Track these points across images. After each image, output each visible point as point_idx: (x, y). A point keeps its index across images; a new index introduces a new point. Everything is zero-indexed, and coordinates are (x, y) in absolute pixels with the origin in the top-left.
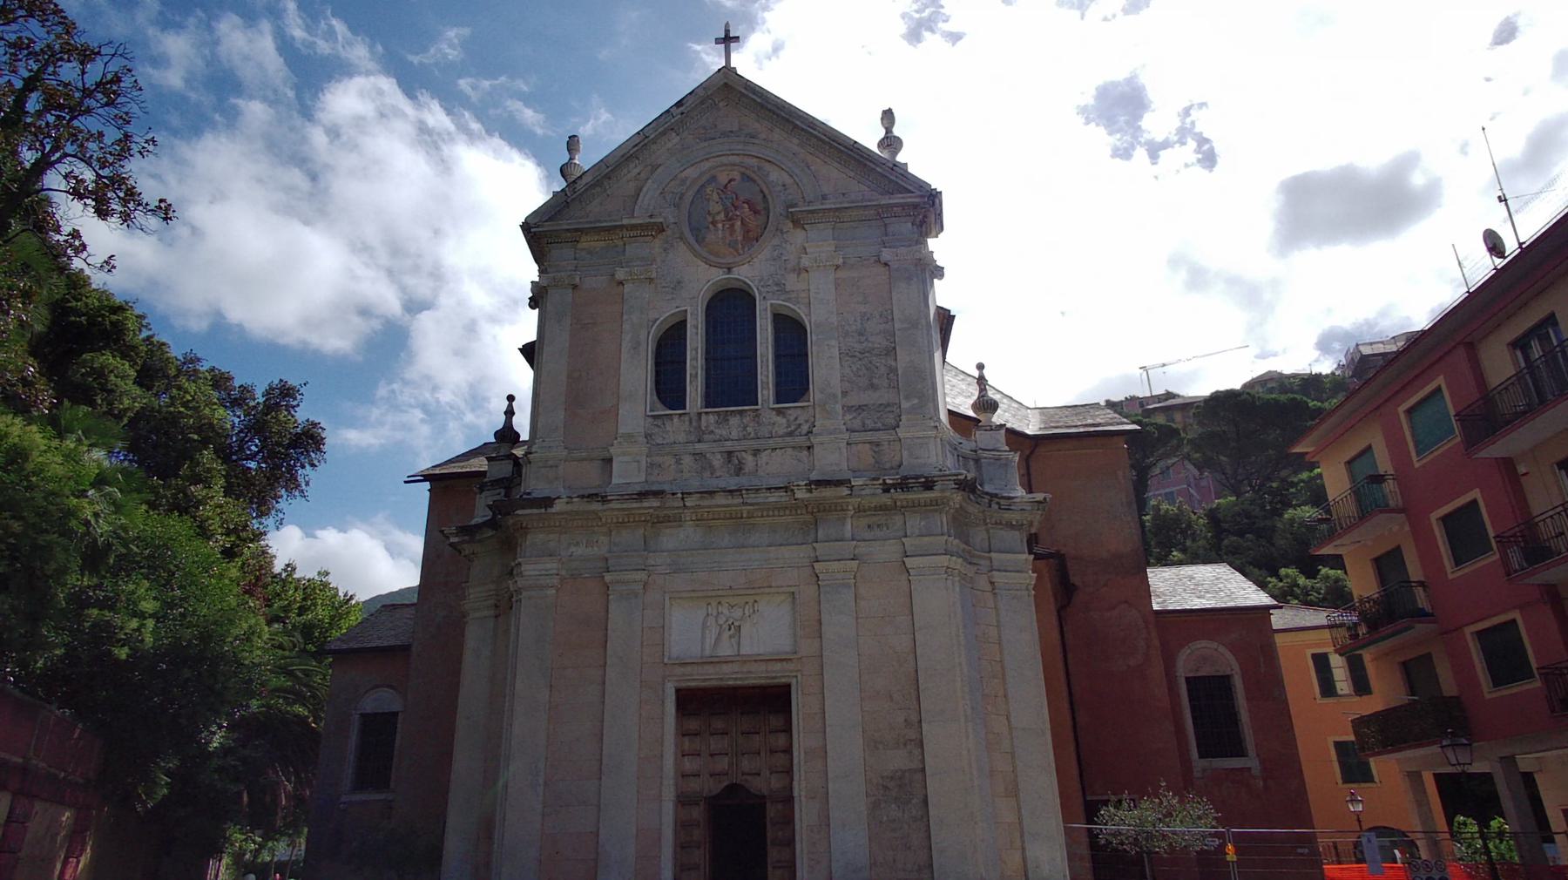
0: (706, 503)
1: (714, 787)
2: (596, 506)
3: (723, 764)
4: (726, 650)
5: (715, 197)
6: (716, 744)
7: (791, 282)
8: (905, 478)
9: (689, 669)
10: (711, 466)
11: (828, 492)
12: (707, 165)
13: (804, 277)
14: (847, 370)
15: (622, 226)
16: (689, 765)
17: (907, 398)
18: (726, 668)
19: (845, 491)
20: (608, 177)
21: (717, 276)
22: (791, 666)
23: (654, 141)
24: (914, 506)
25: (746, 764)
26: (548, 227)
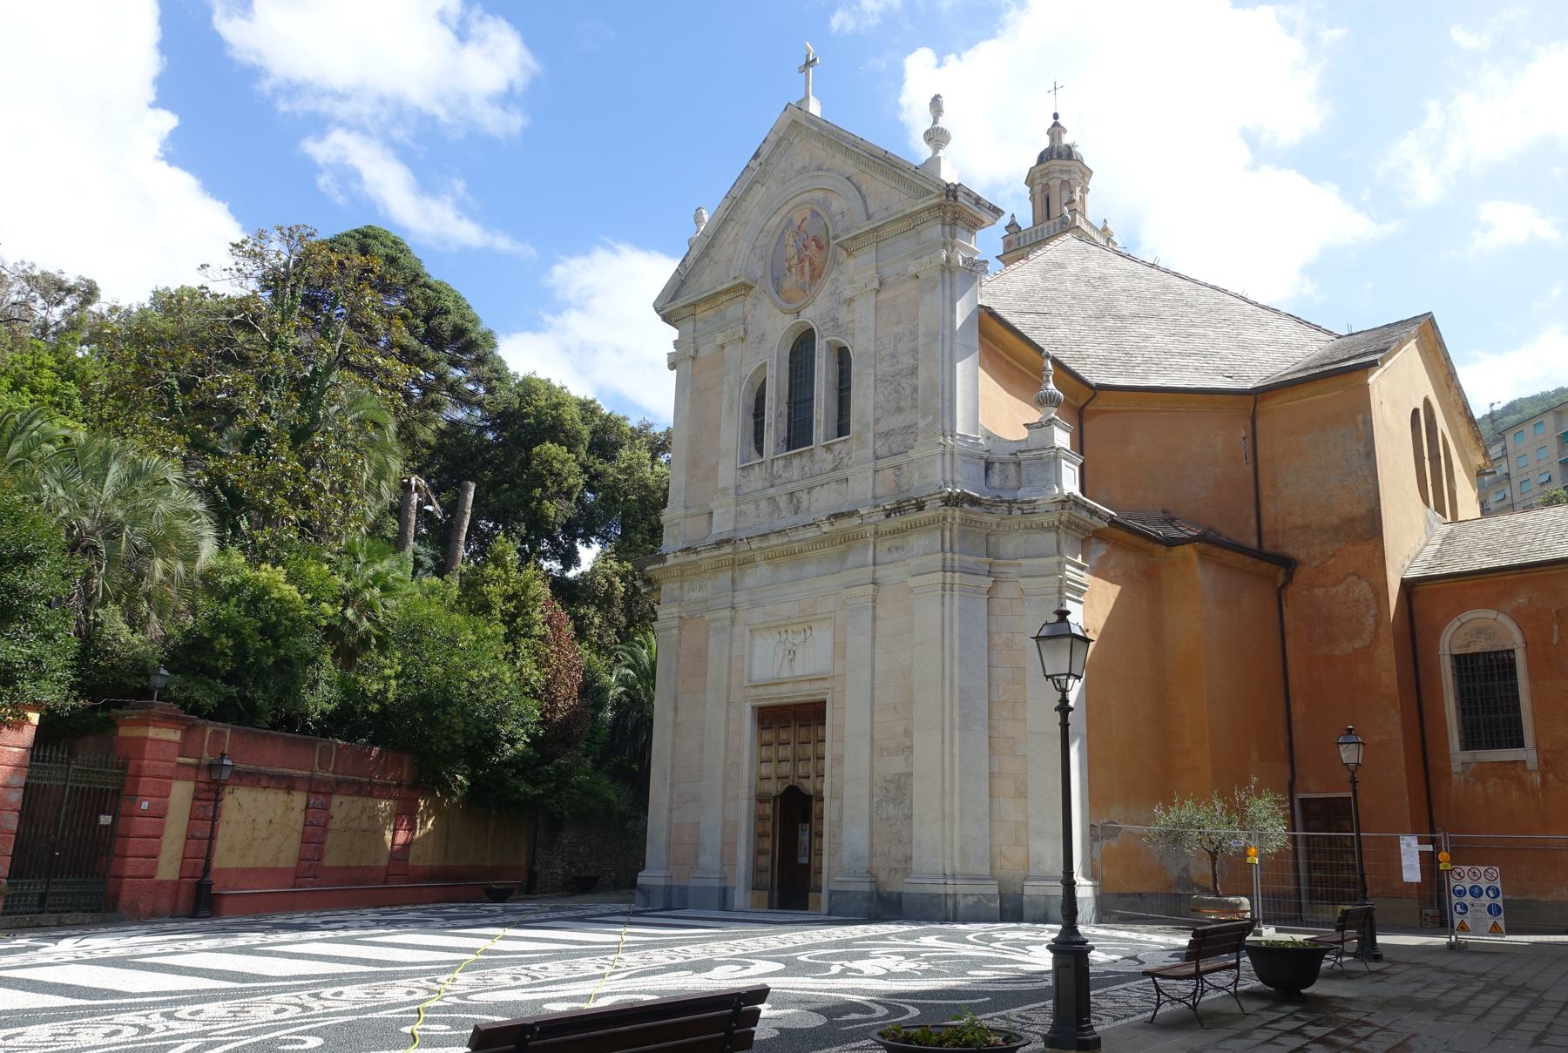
0: (764, 544)
1: (774, 787)
2: (693, 557)
3: (786, 768)
4: (786, 673)
5: (791, 242)
6: (785, 752)
7: (844, 315)
8: (899, 503)
9: (760, 691)
10: (779, 508)
11: (843, 524)
12: (786, 209)
13: (849, 307)
14: (881, 397)
15: (719, 293)
16: (766, 770)
17: (924, 416)
18: (784, 689)
19: (856, 521)
20: (709, 246)
21: (789, 320)
22: (826, 684)
23: (743, 198)
24: (915, 527)
25: (802, 770)
26: (679, 303)
